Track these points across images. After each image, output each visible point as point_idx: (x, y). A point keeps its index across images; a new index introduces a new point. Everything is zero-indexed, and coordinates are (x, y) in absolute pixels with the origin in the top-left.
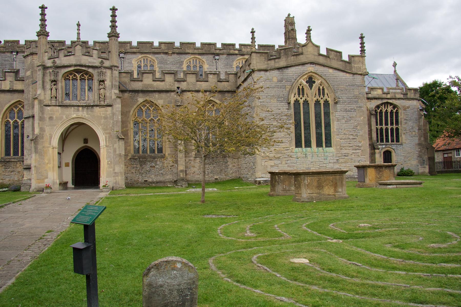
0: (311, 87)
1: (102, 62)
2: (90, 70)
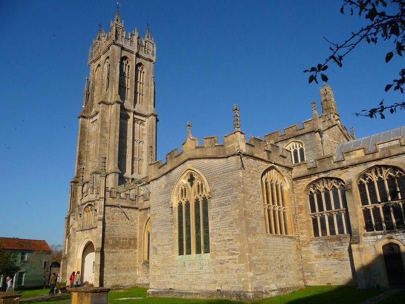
0: (192, 185)
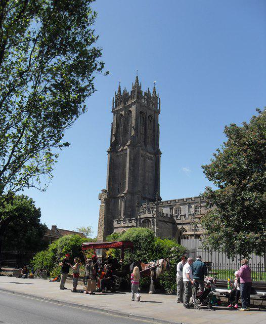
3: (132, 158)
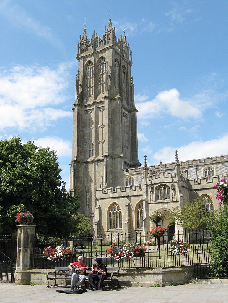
1: (173, 180)
2: (167, 184)
3: (110, 113)
